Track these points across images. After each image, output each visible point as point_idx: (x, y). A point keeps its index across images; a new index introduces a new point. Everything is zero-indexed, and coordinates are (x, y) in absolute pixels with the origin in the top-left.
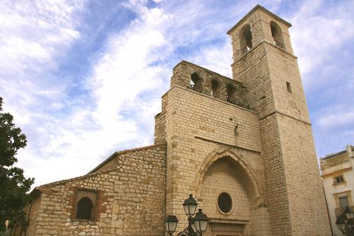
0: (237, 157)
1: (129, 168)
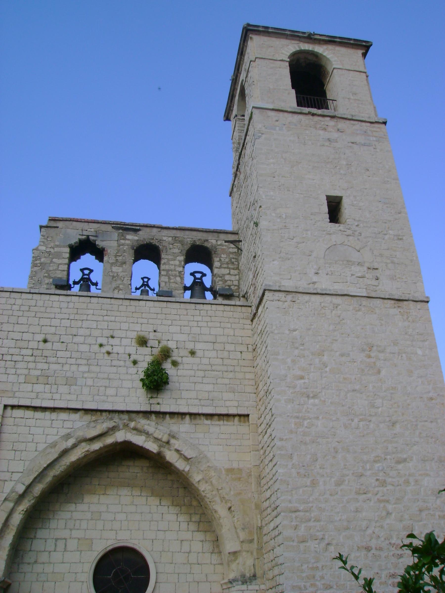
0: (157, 440)
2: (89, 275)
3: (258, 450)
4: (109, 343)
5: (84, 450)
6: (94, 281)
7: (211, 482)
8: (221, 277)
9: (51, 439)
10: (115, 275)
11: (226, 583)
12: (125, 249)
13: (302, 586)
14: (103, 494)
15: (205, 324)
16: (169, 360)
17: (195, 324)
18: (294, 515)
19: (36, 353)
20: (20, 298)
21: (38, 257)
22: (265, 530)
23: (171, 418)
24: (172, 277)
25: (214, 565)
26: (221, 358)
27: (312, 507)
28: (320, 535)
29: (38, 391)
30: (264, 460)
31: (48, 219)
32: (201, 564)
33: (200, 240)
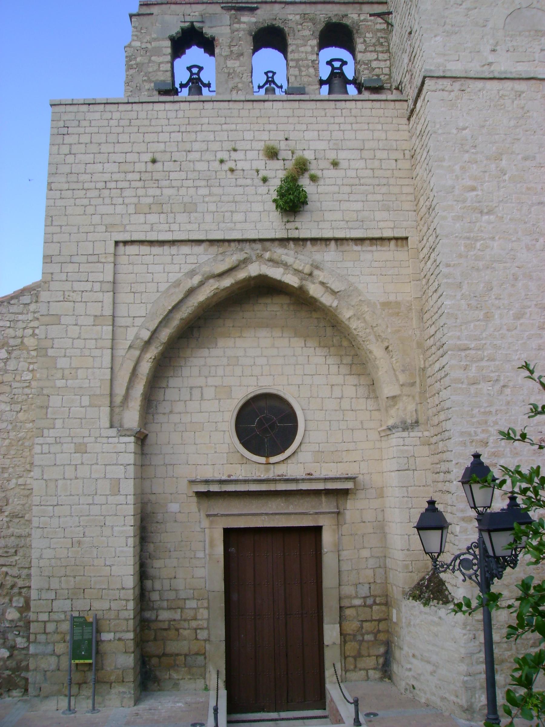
0: (297, 272)
2: (198, 74)
3: (419, 280)
4: (231, 158)
5: (213, 288)
6: (206, 81)
7: (364, 318)
8: (367, 64)
9: (173, 277)
10: (231, 71)
11: (384, 430)
12: (240, 35)
13: (472, 432)
14: (239, 337)
15: (349, 127)
16: (307, 175)
17: (337, 127)
18: (463, 354)
19: (144, 176)
20: (118, 111)
21: (132, 55)
22: (429, 372)
23: (313, 245)
24: (303, 69)
25: (370, 411)
26: (371, 169)
27: (485, 344)
28: (494, 375)
29: (152, 222)
30: (427, 291)
31: (138, 4)
32: (356, 411)
33: (336, 15)
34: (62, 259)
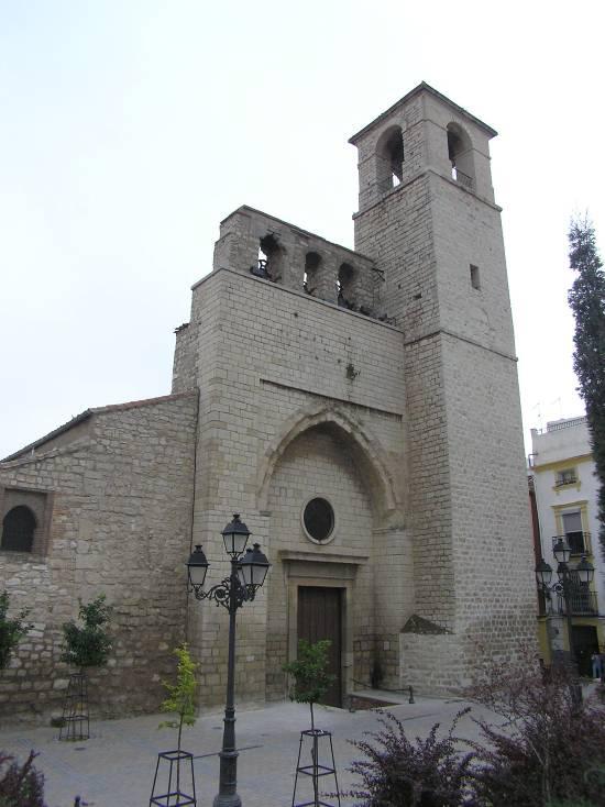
0: (351, 424)
1: (115, 444)
9: (291, 412)
34: (227, 383)
